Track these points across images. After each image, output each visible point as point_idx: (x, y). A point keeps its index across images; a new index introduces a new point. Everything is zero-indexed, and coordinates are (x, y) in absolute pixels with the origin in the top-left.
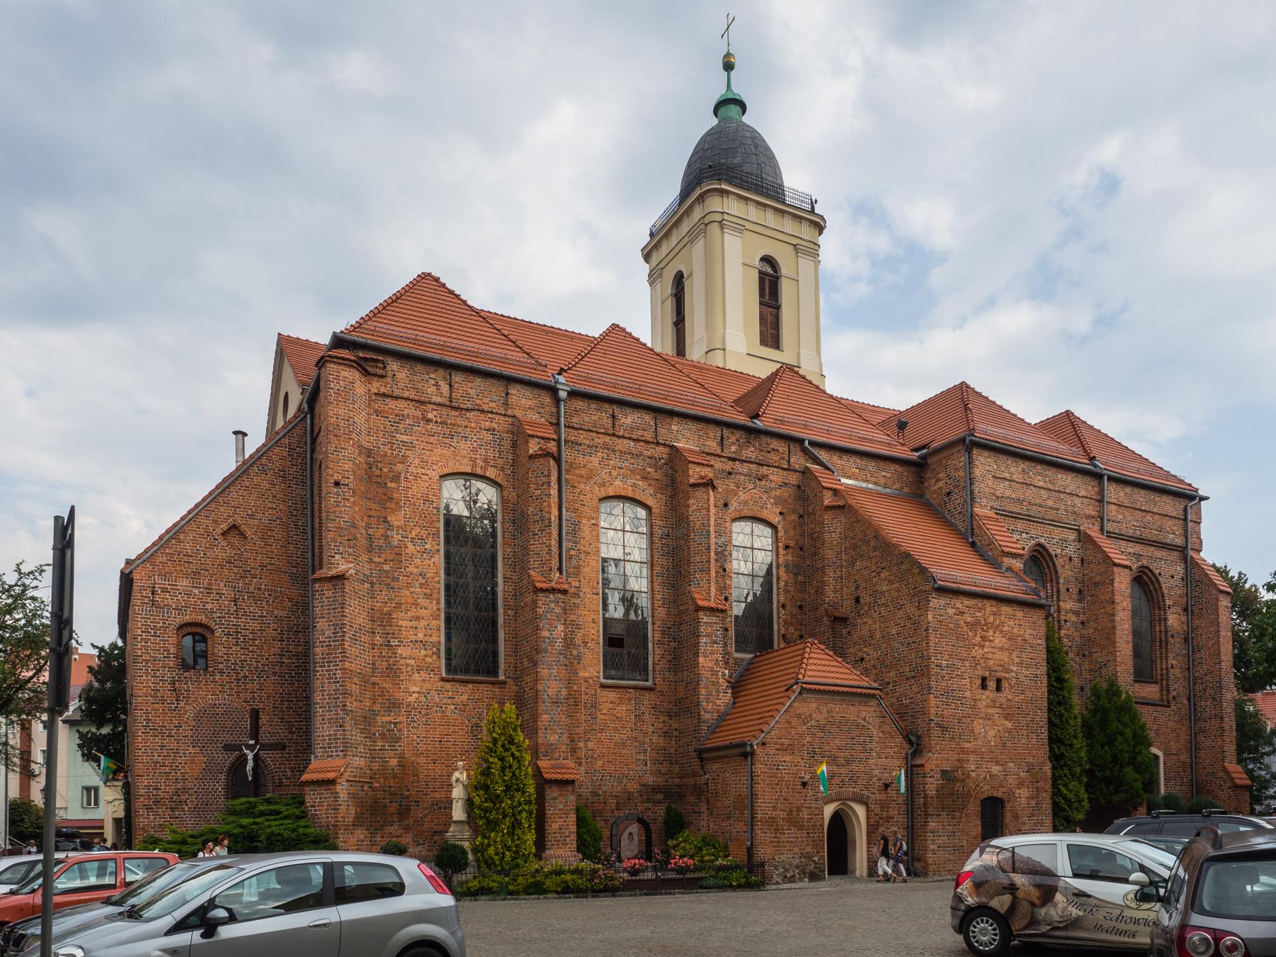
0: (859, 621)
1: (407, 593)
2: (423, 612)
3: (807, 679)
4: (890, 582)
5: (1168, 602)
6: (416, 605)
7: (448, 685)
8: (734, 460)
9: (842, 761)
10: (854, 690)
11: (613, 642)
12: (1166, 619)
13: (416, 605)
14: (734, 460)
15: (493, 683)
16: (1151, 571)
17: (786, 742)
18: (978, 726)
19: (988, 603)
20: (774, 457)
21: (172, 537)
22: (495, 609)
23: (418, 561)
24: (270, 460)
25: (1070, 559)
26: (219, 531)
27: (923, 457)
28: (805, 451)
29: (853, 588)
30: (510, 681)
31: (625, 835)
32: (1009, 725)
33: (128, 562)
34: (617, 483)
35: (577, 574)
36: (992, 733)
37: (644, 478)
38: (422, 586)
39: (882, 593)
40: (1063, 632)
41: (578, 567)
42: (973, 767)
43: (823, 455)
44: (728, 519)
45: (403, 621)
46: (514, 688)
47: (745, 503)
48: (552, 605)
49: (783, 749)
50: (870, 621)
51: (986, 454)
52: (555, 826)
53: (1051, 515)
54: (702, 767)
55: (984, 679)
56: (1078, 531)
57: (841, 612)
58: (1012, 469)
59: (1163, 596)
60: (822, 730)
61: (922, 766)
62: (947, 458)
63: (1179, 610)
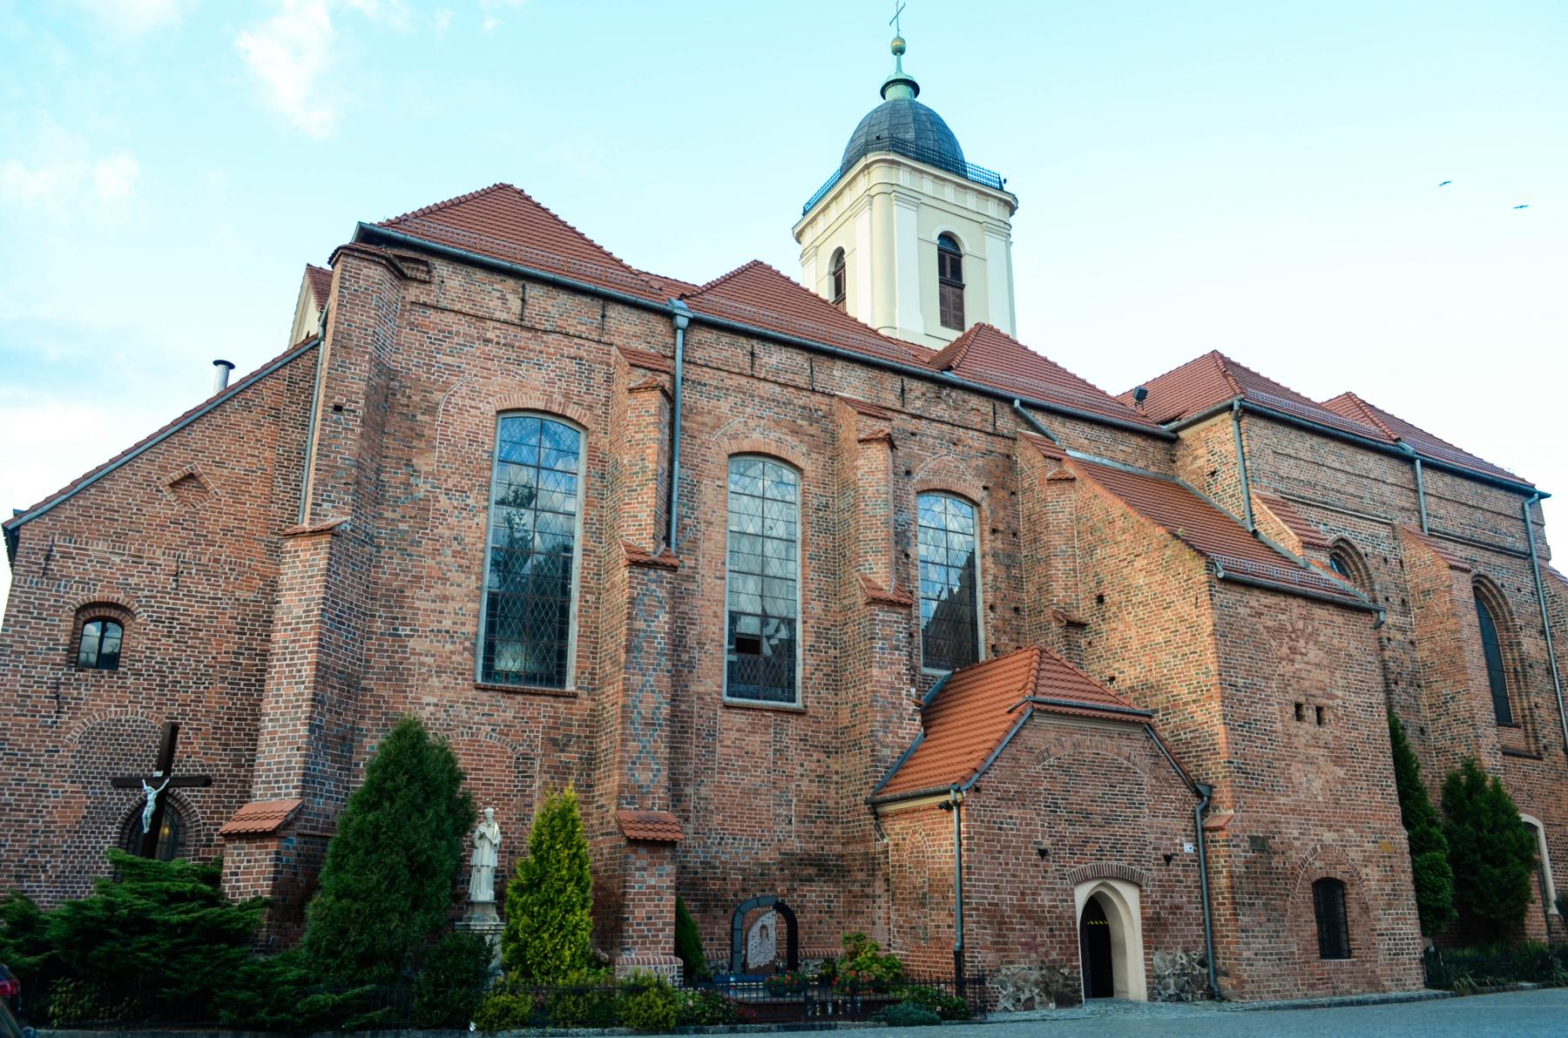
0: (1105, 627)
1: (429, 562)
2: (452, 591)
3: (1039, 697)
4: (1150, 573)
5: (1518, 622)
6: (444, 580)
7: (484, 696)
8: (919, 417)
9: (1099, 819)
10: (1112, 715)
11: (745, 645)
12: (1519, 644)
13: (444, 580)
14: (919, 417)
15: (556, 696)
16: (1492, 582)
17: (1013, 788)
18: (1297, 773)
19: (1294, 603)
20: (974, 419)
21: (91, 485)
22: (566, 592)
23: (452, 521)
24: (258, 393)
25: (1385, 560)
26: (167, 480)
27: (1175, 431)
28: (1016, 412)
29: (1093, 584)
30: (583, 694)
31: (756, 929)
32: (1341, 773)
33: (18, 514)
34: (756, 435)
35: (692, 550)
36: (1317, 784)
37: (794, 432)
38: (455, 554)
39: (1139, 588)
40: (1387, 654)
41: (695, 541)
42: (1296, 833)
43: (1040, 419)
44: (912, 492)
45: (421, 601)
46: (589, 704)
47: (935, 472)
48: (653, 586)
49: (1006, 799)
50: (1121, 627)
51: (1262, 423)
52: (640, 913)
53: (1353, 503)
54: (878, 827)
55: (1298, 706)
56: (1393, 528)
57: (1078, 615)
58: (1297, 445)
59: (1511, 613)
60: (1066, 772)
61: (1221, 829)
62: (1208, 430)
63: (1534, 632)
